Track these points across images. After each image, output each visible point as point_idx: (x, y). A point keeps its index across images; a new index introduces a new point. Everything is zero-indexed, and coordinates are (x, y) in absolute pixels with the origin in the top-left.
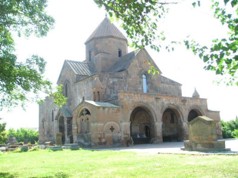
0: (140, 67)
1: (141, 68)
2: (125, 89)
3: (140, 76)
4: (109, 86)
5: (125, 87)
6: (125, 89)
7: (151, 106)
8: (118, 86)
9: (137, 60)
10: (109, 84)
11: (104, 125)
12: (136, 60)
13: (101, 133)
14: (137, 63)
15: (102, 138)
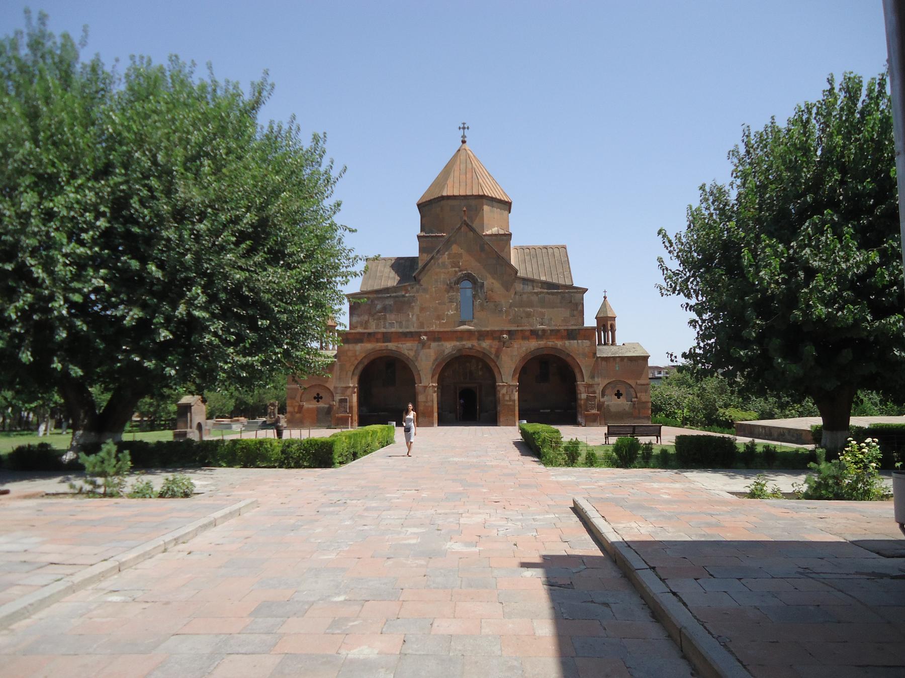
1: (457, 269)
6: (411, 316)
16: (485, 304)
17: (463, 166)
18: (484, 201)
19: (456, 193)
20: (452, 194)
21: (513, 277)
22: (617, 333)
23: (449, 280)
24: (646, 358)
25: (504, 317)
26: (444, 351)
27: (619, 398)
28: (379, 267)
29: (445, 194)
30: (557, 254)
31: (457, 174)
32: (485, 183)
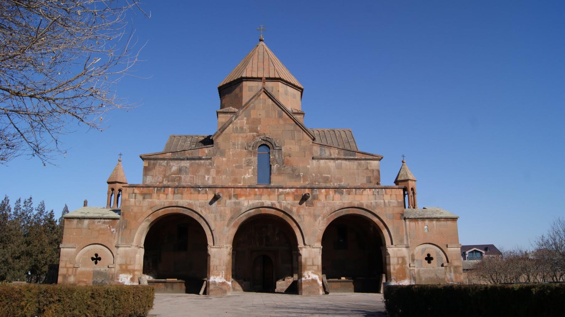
0: (252, 130)
1: (255, 134)
2: (208, 178)
3: (251, 149)
4: (168, 177)
5: (207, 177)
6: (206, 179)
7: (201, 211)
8: (190, 175)
9: (245, 118)
10: (167, 175)
11: (76, 254)
12: (242, 119)
13: (68, 266)
14: (245, 123)
15: (70, 276)
16: (283, 169)
17: (261, 57)
18: (280, 84)
19: (255, 75)
20: (251, 76)
21: (311, 143)
22: (417, 196)
23: (247, 144)
24: (454, 219)
25: (302, 182)
26: (240, 210)
27: (429, 262)
28: (180, 142)
29: (244, 75)
30: (343, 135)
31: (255, 61)
32: (281, 70)
